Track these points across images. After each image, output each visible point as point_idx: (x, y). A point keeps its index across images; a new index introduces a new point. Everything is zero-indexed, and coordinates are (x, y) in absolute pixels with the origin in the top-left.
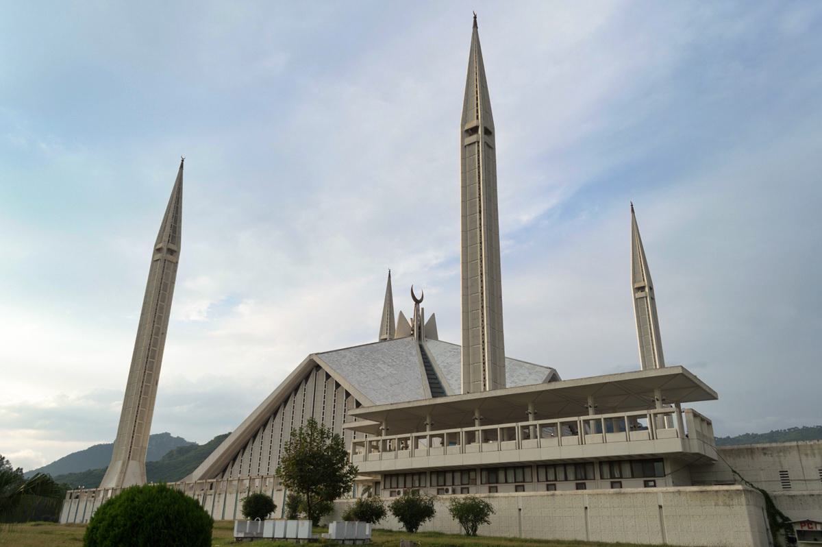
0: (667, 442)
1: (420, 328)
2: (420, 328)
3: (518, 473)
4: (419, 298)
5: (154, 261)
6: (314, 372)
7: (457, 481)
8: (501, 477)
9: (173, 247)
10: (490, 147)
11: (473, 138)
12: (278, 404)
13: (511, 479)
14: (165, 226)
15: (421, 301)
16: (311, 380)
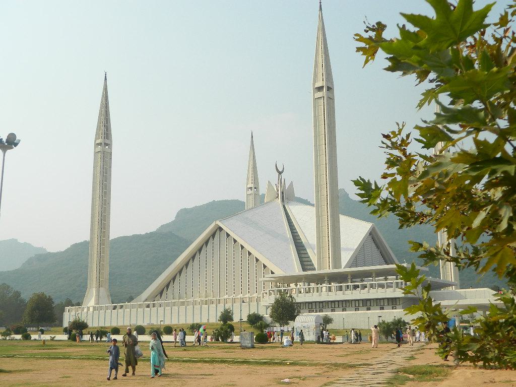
0: (399, 293)
1: (283, 192)
2: (282, 193)
3: (344, 305)
4: (280, 170)
5: (96, 153)
6: (218, 232)
7: (318, 307)
8: (337, 306)
9: (107, 141)
10: (331, 99)
11: (319, 94)
12: (195, 252)
13: (341, 306)
14: (100, 127)
15: (283, 171)
16: (217, 236)
